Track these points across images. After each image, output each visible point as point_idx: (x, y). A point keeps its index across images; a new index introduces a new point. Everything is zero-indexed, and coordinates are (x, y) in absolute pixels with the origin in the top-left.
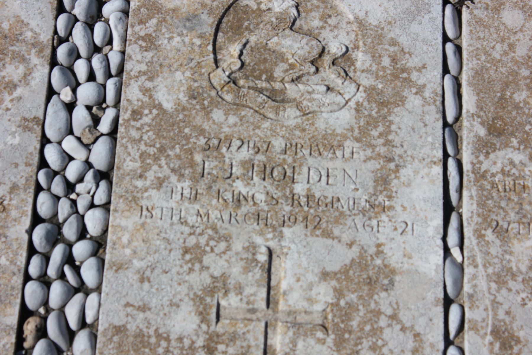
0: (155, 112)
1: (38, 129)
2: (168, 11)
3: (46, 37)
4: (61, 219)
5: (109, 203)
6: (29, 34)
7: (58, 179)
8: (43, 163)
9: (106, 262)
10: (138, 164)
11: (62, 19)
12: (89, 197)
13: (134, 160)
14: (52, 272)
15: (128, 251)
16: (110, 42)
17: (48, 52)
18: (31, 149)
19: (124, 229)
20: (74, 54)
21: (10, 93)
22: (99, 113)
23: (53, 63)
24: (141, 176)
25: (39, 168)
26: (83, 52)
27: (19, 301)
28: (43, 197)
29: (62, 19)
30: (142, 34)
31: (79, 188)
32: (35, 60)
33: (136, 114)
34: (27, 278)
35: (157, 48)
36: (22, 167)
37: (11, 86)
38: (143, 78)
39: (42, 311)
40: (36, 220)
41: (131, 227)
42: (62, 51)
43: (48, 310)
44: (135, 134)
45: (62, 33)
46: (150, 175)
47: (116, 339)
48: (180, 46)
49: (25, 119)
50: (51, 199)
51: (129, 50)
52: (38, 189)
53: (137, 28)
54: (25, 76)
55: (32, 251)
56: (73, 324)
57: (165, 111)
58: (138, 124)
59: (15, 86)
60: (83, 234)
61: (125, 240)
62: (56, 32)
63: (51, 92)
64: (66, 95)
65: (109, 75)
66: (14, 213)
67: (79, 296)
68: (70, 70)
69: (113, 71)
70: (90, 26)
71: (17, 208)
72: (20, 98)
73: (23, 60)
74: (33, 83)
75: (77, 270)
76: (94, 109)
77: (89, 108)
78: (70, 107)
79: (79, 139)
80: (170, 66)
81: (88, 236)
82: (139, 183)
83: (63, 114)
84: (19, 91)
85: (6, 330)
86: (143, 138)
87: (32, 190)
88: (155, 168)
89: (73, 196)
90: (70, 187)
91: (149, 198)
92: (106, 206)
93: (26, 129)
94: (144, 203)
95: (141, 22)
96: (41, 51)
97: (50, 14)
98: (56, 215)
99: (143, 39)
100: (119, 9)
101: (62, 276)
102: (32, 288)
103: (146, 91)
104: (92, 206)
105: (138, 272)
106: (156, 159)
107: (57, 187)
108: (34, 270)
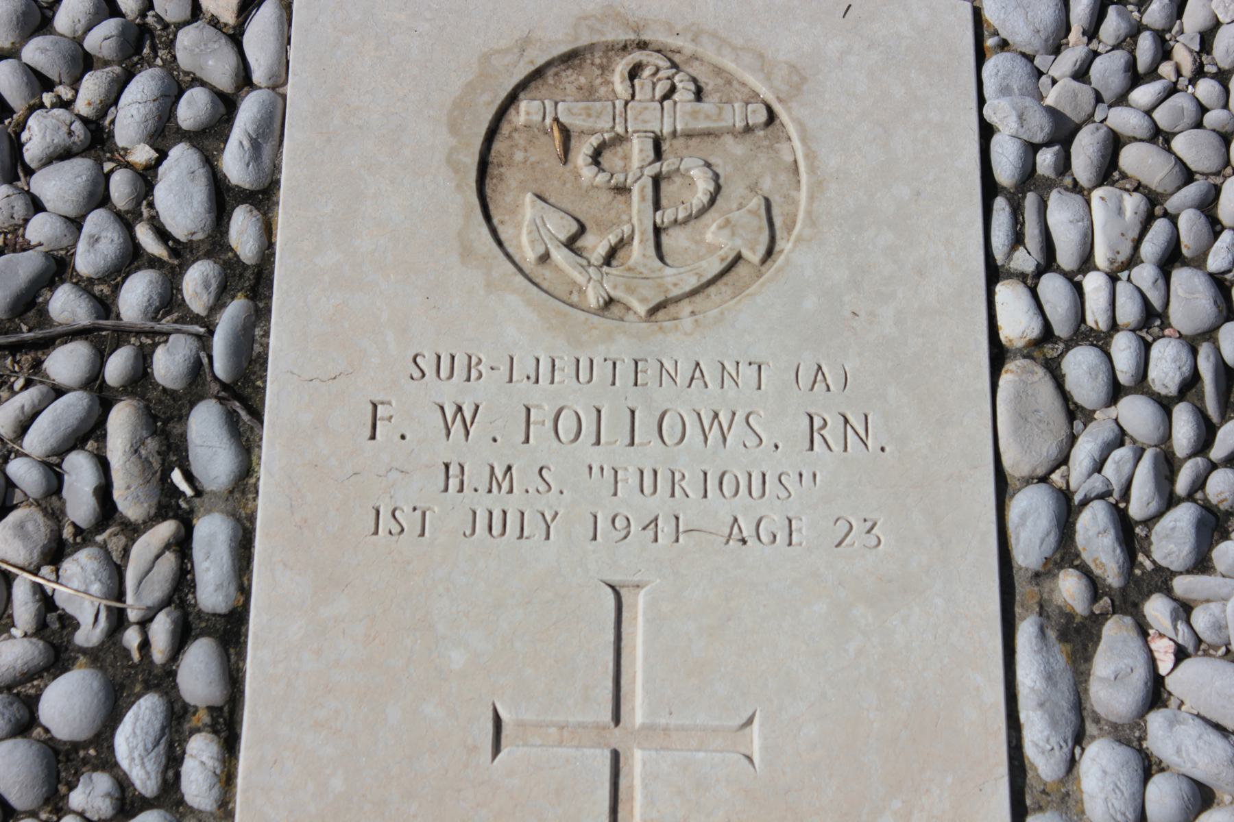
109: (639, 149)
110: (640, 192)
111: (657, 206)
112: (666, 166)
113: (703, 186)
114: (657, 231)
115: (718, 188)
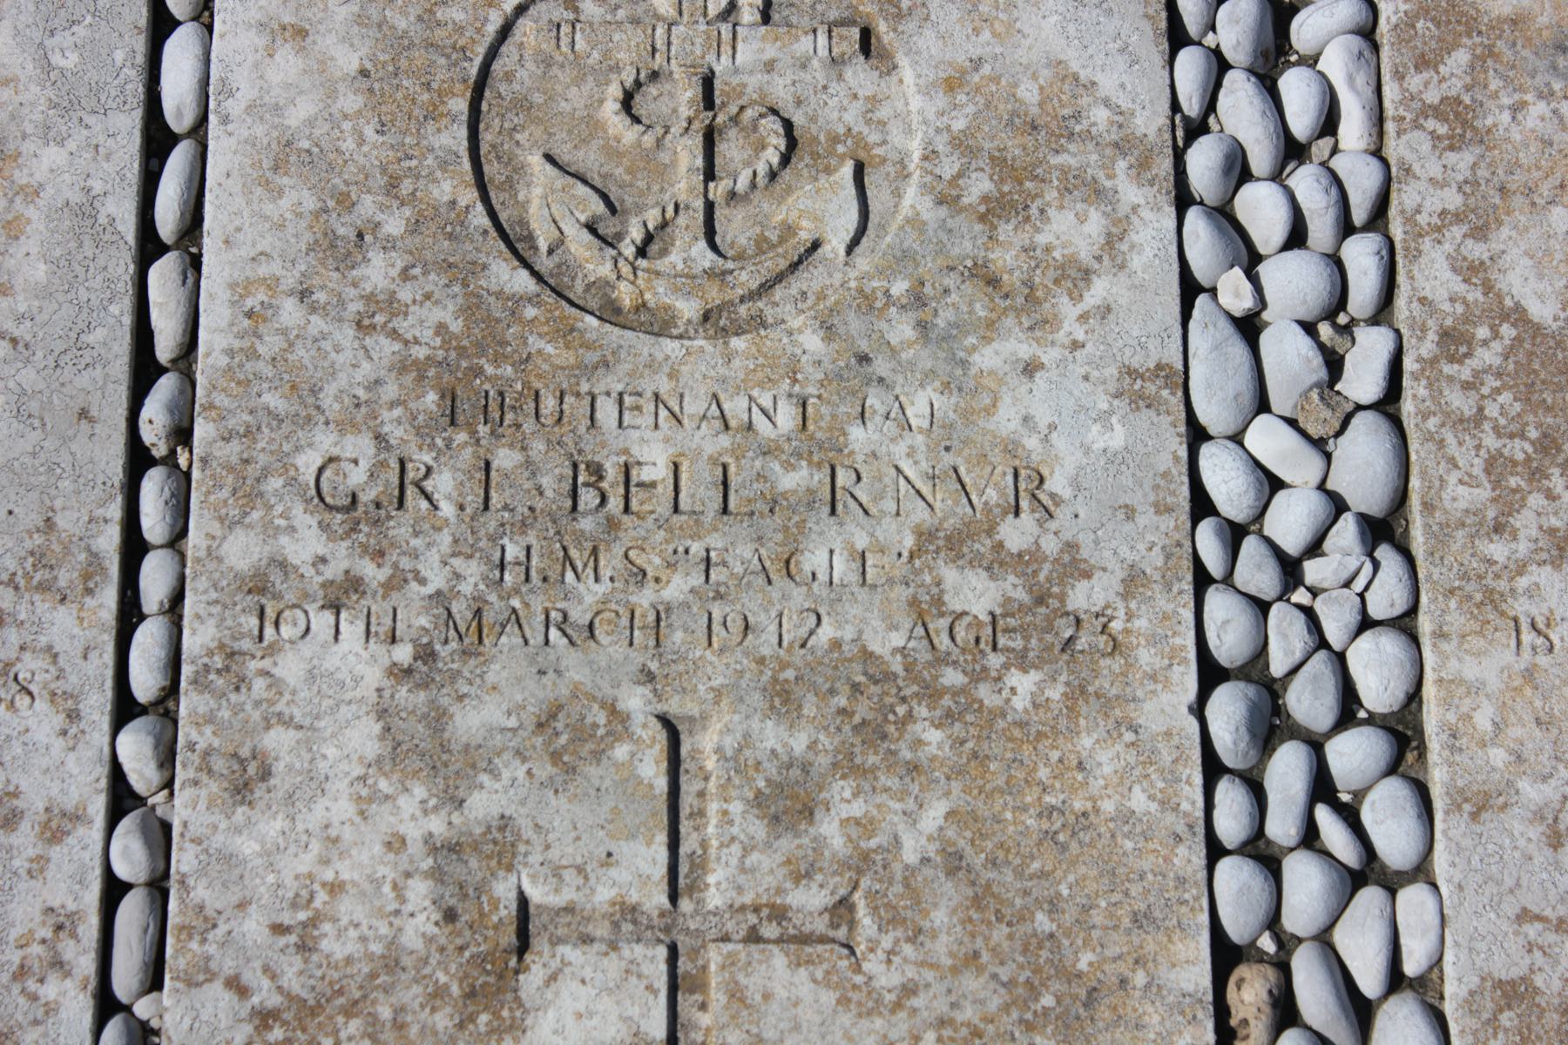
0: (1507, 331)
1: (1176, 401)
2: (1497, 25)
3: (1151, 122)
4: (1278, 666)
5: (1413, 610)
6: (1101, 115)
7: (1250, 545)
8: (1202, 505)
9: (1436, 792)
10: (1484, 493)
11: (1190, 64)
12: (1350, 596)
13: (1469, 481)
14: (1282, 827)
15: (1498, 756)
16: (1329, 123)
17: (1165, 165)
18: (1164, 462)
19: (1475, 689)
20: (1238, 170)
21: (1076, 297)
22: (1340, 344)
23: (1183, 200)
24: (1498, 529)
25: (1195, 520)
26: (1261, 157)
27: (1204, 918)
28: (1218, 604)
29: (1190, 64)
30: (1432, 97)
31: (1313, 570)
32: (1130, 193)
33: (1454, 342)
34: (1215, 851)
35: (1483, 138)
36: (1146, 518)
37: (1076, 276)
38: (1457, 231)
39: (1267, 944)
40: (1211, 674)
41: (1494, 683)
42: (1203, 162)
43: (1287, 943)
44: (1458, 401)
45: (1192, 105)
46: (1526, 522)
47: (1506, 1018)
48: (1549, 129)
49: (1132, 373)
50: (1249, 610)
51: (1395, 149)
52: (1202, 580)
53: (1415, 81)
54: (1112, 241)
55: (1213, 768)
56: (1370, 982)
57: (1537, 329)
58: (1466, 374)
59: (1087, 274)
60: (1349, 710)
61: (1483, 720)
62: (1175, 106)
63: (1190, 289)
64: (1237, 295)
65: (1347, 229)
66: (1146, 657)
67: (1370, 898)
68: (1224, 214)
69: (1359, 216)
70: (1267, 82)
71: (1153, 641)
72: (1106, 310)
73: (1098, 194)
74: (1136, 263)
75: (1350, 816)
76: (1325, 330)
77: (1309, 328)
78: (1249, 327)
79: (1292, 422)
80: (1530, 191)
81: (1362, 714)
82: (1498, 550)
83: (1238, 350)
84: (1099, 291)
85: (1182, 1006)
86: (1487, 412)
87: (1187, 585)
88: (1536, 500)
89: (1301, 596)
90: (1290, 569)
91: (1533, 592)
92: (1405, 624)
93: (1141, 401)
94: (1521, 607)
95: (1422, 63)
96: (1143, 164)
97: (1152, 49)
98: (1262, 651)
99: (1437, 112)
100: (1350, 26)
101: (1310, 837)
102: (1235, 876)
103: (1471, 271)
104: (1366, 623)
105: (1539, 816)
106: (1536, 475)
107: (1257, 573)
108: (1231, 822)
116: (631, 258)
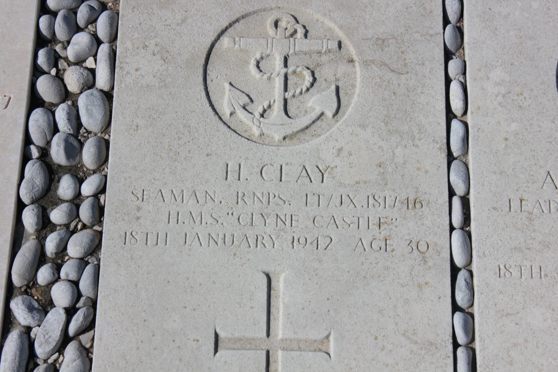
109: (278, 62)
110: (279, 83)
111: (286, 89)
112: (290, 69)
113: (309, 79)
114: (286, 101)
115: (315, 79)
116: (259, 119)
